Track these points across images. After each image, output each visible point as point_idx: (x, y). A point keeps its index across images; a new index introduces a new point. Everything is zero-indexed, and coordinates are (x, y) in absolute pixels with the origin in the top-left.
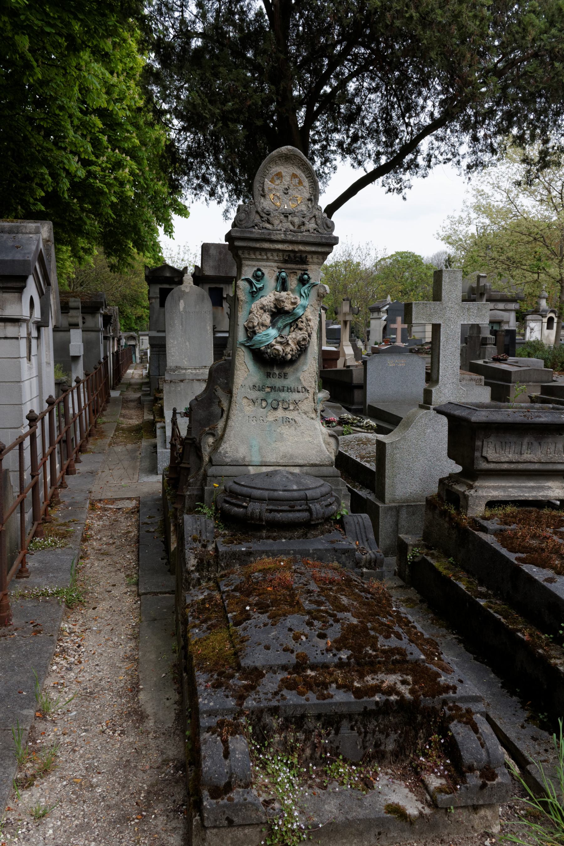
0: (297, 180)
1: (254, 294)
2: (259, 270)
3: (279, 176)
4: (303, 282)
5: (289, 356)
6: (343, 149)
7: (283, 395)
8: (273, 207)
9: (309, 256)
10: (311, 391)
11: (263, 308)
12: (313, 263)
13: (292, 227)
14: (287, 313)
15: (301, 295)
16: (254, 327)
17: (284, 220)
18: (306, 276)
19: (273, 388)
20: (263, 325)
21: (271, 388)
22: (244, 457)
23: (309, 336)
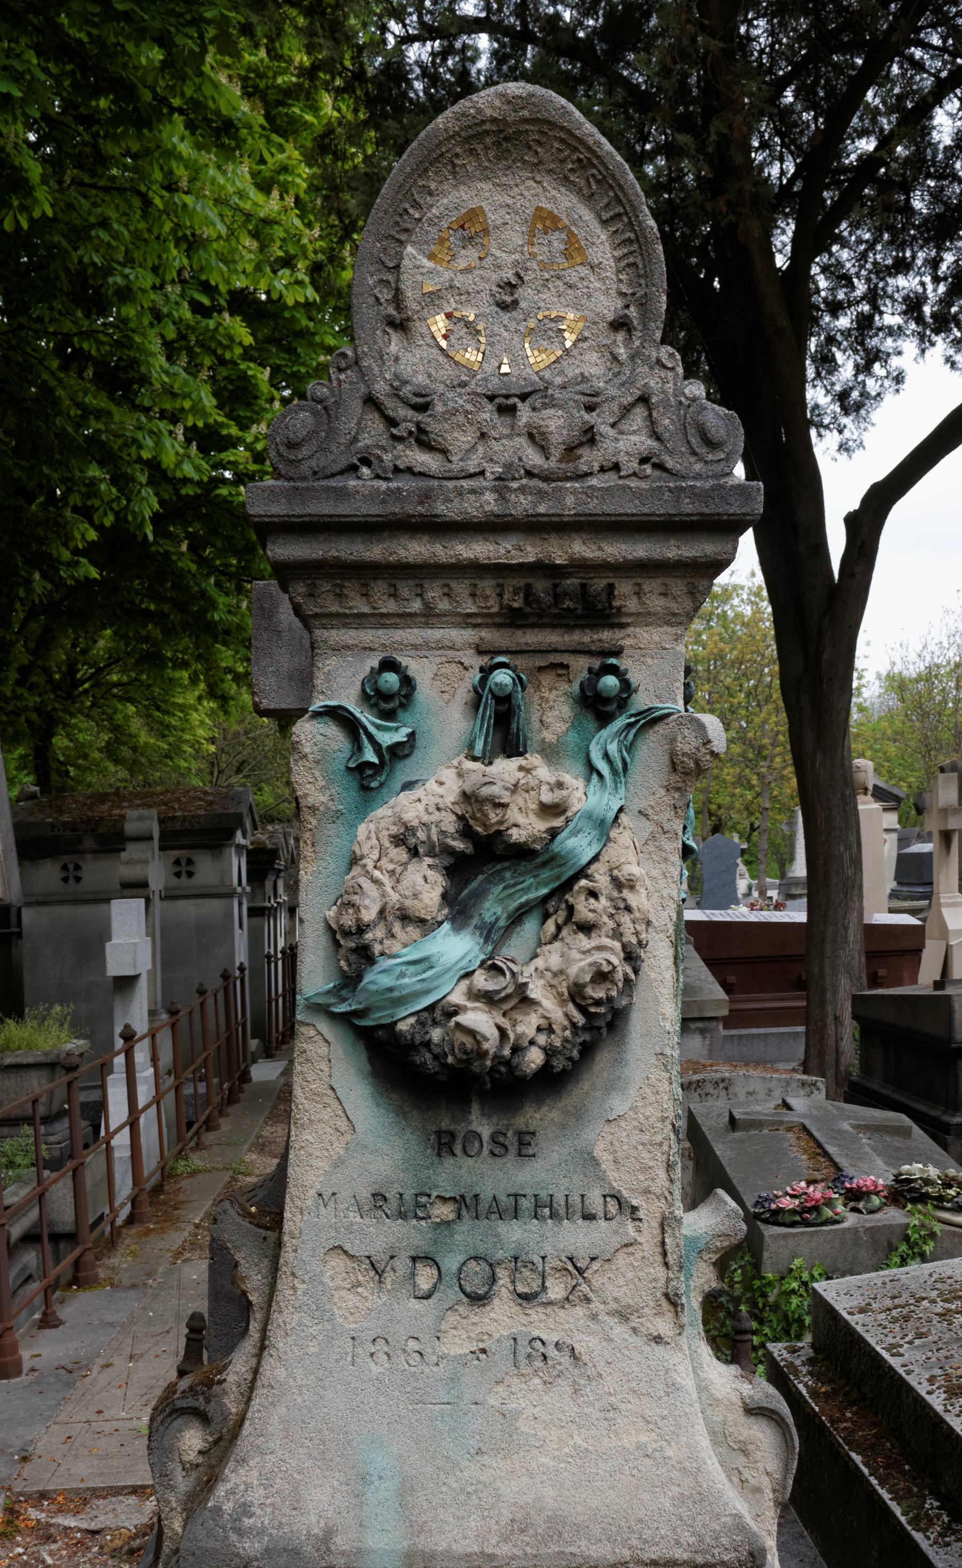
0: (557, 241)
1: (370, 777)
2: (389, 665)
3: (472, 229)
4: (597, 707)
5: (534, 1058)
6: (920, 320)
7: (515, 1233)
8: (447, 372)
9: (624, 588)
10: (650, 1211)
11: (404, 838)
12: (646, 618)
13: (534, 458)
14: (522, 854)
15: (591, 769)
16: (362, 929)
17: (501, 426)
18: (610, 682)
19: (466, 1204)
20: (405, 918)
21: (460, 1202)
22: (329, 1533)
23: (630, 957)
